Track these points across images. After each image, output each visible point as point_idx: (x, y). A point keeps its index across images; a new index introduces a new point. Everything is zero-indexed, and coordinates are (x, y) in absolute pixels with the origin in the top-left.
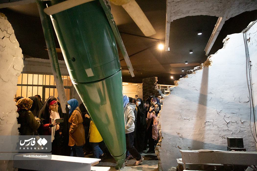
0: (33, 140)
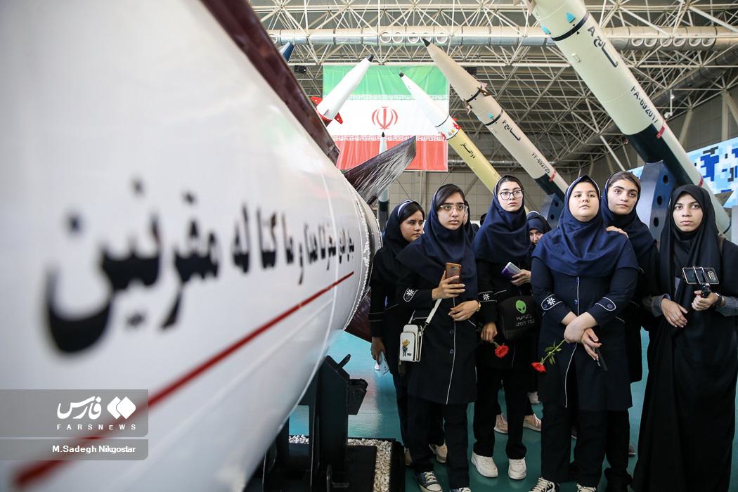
0: (95, 402)
